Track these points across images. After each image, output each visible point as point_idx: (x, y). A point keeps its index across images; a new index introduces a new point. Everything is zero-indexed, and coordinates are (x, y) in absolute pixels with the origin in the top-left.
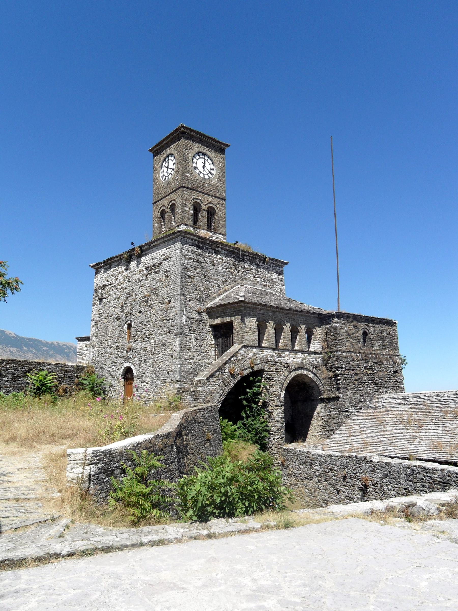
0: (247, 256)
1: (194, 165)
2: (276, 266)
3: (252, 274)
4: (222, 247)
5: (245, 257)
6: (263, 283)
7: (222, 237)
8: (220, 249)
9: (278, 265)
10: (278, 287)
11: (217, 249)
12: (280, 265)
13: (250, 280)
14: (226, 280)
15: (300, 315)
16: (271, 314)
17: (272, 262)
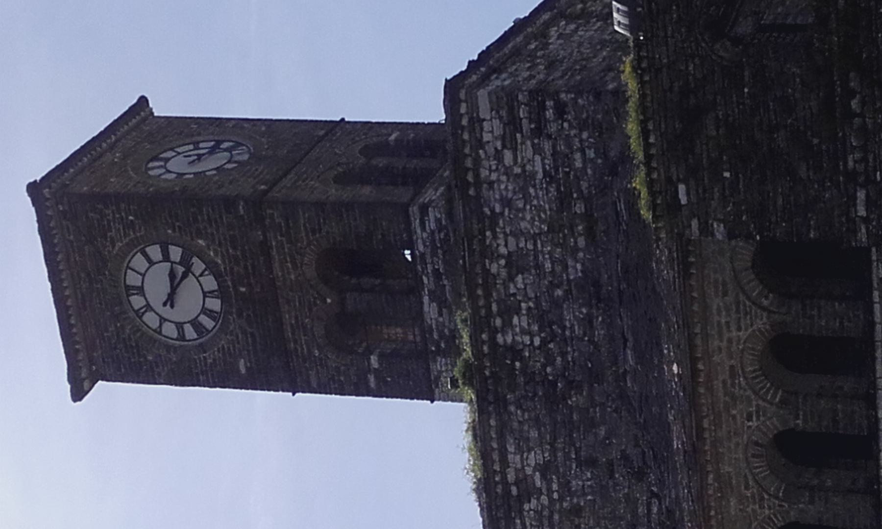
0: (494, 332)
1: (190, 332)
2: (480, 144)
3: (557, 304)
4: (497, 467)
5: (500, 339)
6: (581, 242)
7: (423, 229)
8: (511, 477)
9: (472, 131)
10: (577, 144)
11: (514, 490)
12: (471, 120)
13: (588, 321)
14: (625, 457)
15: (706, 337)
16: (733, 502)
17: (470, 178)
